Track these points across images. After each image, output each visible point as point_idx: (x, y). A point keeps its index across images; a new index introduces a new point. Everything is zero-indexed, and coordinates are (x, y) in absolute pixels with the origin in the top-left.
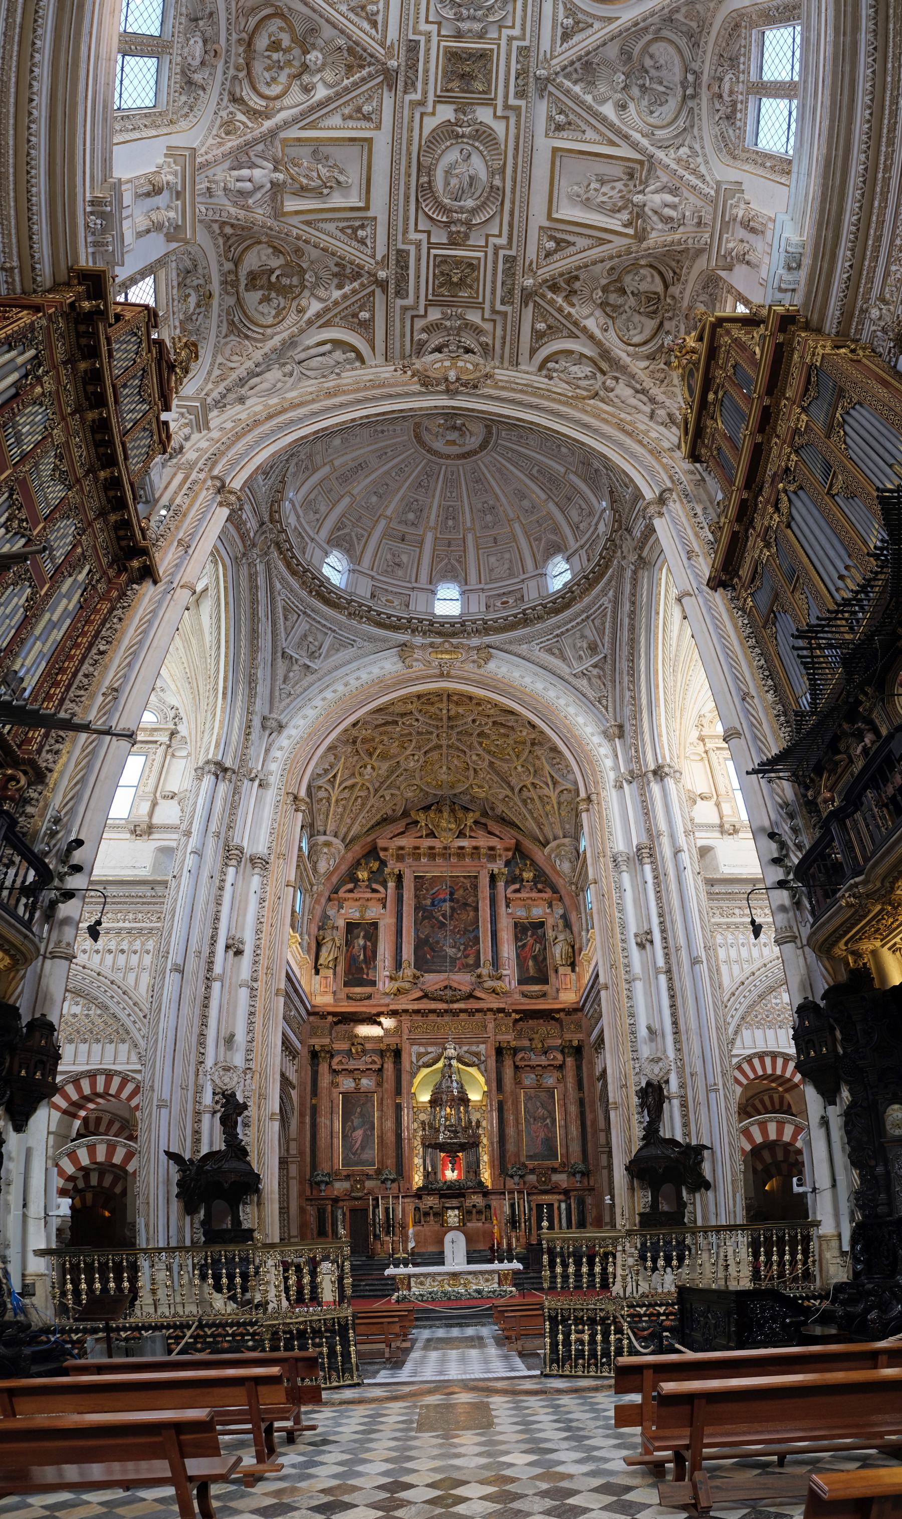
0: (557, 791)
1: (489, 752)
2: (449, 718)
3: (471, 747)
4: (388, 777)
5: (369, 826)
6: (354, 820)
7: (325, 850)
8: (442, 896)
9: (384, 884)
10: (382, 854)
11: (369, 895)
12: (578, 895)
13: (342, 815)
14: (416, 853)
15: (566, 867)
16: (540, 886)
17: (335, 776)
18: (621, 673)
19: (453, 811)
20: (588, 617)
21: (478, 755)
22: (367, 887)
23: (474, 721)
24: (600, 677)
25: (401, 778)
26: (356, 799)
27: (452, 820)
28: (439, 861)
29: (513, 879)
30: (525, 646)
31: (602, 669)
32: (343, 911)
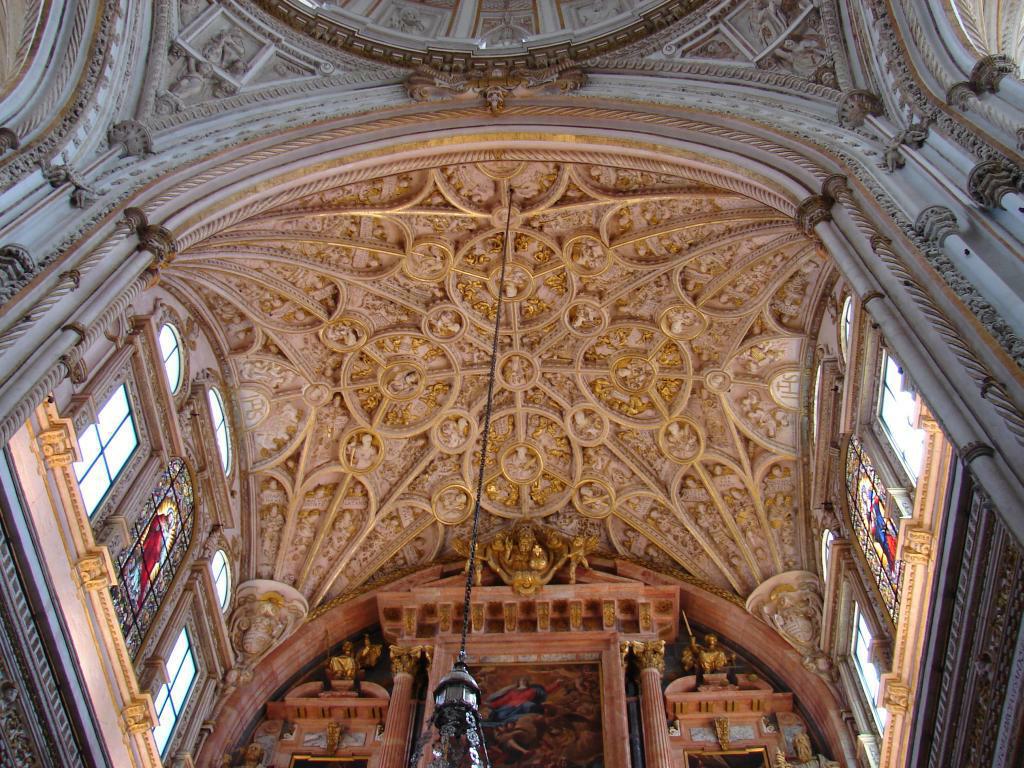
0: (761, 470)
1: (610, 405)
2: (524, 323)
3: (574, 396)
4: (406, 472)
5: (365, 577)
6: (333, 562)
7: (268, 608)
8: (516, 703)
9: (389, 686)
10: (387, 627)
11: (351, 702)
12: (836, 678)
13: (309, 547)
14: (461, 619)
15: (796, 630)
16: (741, 678)
17: (296, 457)
18: (855, 19)
19: (542, 540)
21: (588, 413)
22: (350, 690)
23: (572, 318)
24: (812, 52)
25: (432, 478)
26: (341, 514)
27: (538, 550)
28: (511, 633)
29: (676, 668)
30: (654, 57)
31: (811, 37)
32: (291, 738)
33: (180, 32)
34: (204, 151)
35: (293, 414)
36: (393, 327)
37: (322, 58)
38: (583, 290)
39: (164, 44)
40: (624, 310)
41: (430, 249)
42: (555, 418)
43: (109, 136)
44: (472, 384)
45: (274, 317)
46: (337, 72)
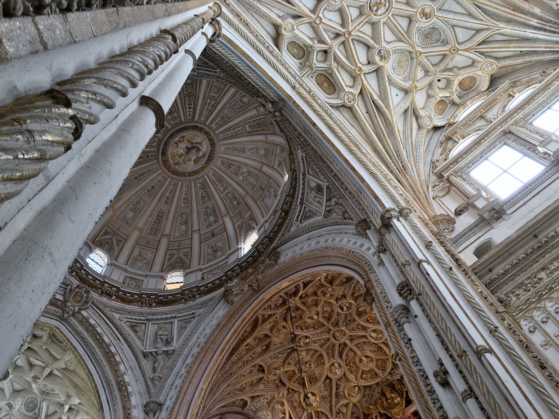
2: (328, 319)
20: (304, 174)
21: (374, 331)
23: (342, 309)
33: (143, 345)
34: (178, 389)
35: (279, 407)
36: (288, 356)
37: (194, 310)
38: (337, 300)
39: (141, 356)
40: (356, 295)
41: (278, 328)
42: (365, 340)
43: (145, 412)
44: (329, 350)
45: (247, 389)
46: (202, 310)
